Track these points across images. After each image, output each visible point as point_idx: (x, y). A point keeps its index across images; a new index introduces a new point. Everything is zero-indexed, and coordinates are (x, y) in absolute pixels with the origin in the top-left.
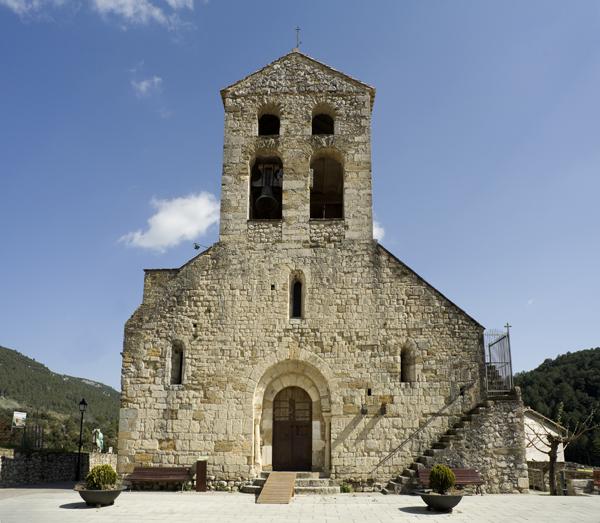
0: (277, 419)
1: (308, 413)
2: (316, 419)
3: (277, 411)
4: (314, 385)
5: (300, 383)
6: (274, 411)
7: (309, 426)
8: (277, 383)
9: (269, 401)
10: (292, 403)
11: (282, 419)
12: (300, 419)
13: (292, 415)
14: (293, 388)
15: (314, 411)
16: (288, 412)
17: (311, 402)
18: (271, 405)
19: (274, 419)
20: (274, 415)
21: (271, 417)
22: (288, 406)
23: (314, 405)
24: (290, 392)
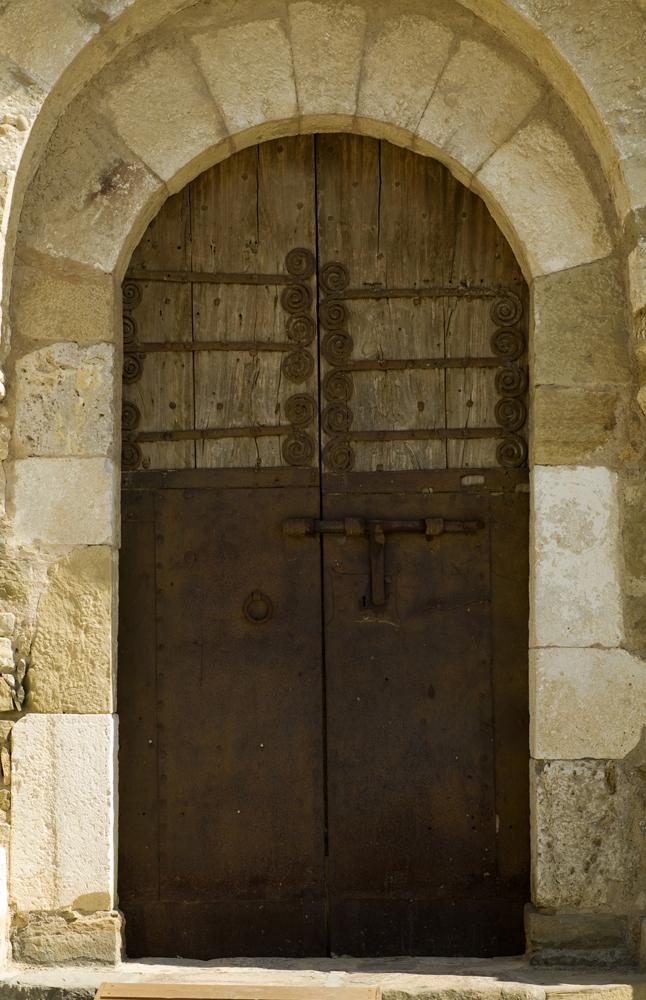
0: (164, 457)
1: (476, 398)
2: (575, 451)
3: (165, 377)
4: (551, 108)
5: (405, 95)
6: (131, 368)
7: (502, 521)
8: (159, 80)
9: (73, 273)
10: (319, 298)
11: (214, 454)
12: (400, 457)
13: (325, 413)
14: (323, 151)
15: (558, 368)
16: (270, 388)
17: (512, 291)
18: (101, 309)
19: (129, 455)
20: (129, 414)
21: (105, 433)
22: (274, 323)
23: (540, 318)
24: (290, 194)
